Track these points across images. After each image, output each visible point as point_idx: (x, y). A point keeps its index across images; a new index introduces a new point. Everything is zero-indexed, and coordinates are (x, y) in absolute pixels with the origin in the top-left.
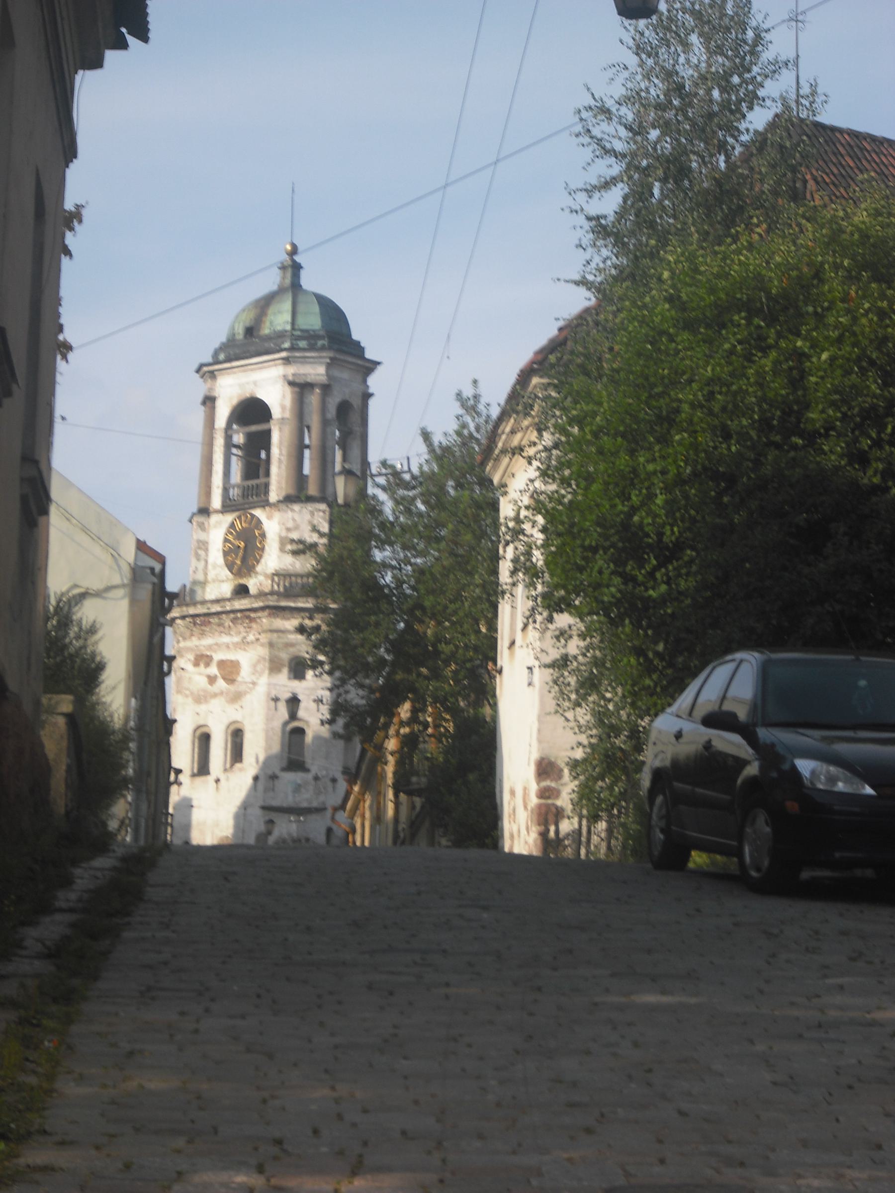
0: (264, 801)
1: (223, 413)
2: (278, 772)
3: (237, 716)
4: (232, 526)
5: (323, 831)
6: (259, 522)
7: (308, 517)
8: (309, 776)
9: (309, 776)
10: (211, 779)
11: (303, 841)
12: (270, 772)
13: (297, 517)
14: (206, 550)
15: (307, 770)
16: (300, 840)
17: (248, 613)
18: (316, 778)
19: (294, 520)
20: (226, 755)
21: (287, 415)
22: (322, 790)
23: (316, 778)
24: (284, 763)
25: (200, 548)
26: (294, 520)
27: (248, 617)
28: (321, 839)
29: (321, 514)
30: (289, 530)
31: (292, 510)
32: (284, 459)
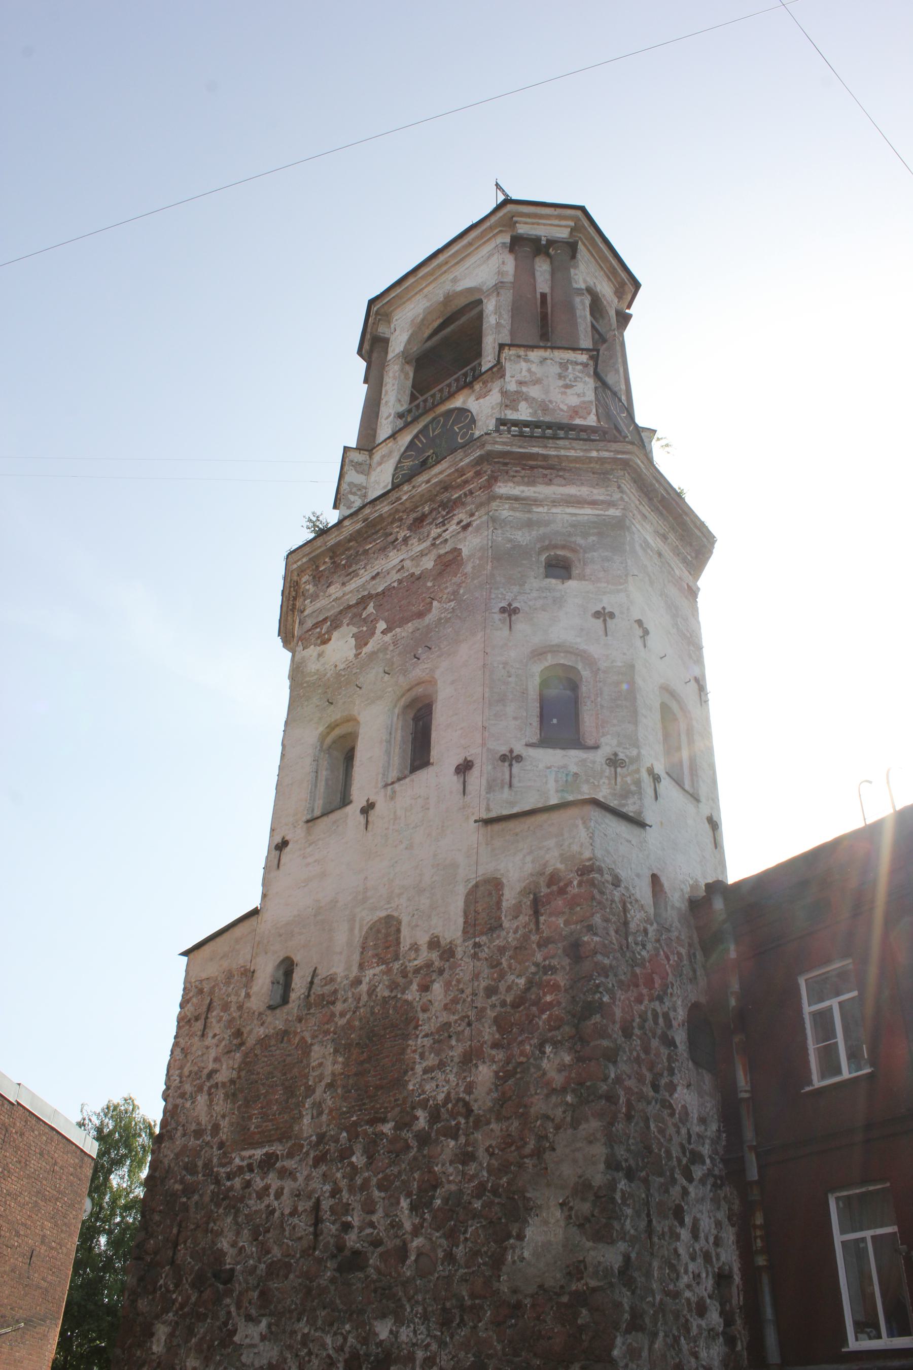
0: (488, 809)
1: (399, 340)
2: (519, 749)
3: (419, 672)
4: (411, 445)
5: (647, 875)
6: (463, 412)
7: (557, 369)
8: (599, 757)
9: (599, 757)
10: (353, 811)
11: (608, 877)
12: (504, 750)
13: (534, 368)
14: (365, 496)
15: (596, 747)
16: (600, 871)
17: (444, 496)
18: (614, 762)
19: (529, 370)
20: (388, 753)
21: (510, 278)
22: (633, 788)
23: (614, 762)
24: (533, 733)
25: (354, 494)
26: (529, 370)
27: (443, 505)
28: (643, 892)
29: (579, 367)
30: (521, 383)
31: (527, 360)
32: (506, 320)
